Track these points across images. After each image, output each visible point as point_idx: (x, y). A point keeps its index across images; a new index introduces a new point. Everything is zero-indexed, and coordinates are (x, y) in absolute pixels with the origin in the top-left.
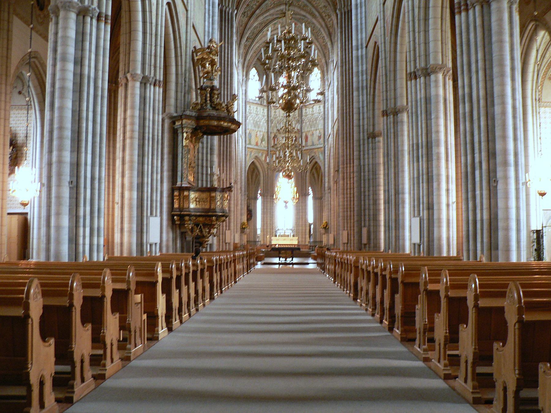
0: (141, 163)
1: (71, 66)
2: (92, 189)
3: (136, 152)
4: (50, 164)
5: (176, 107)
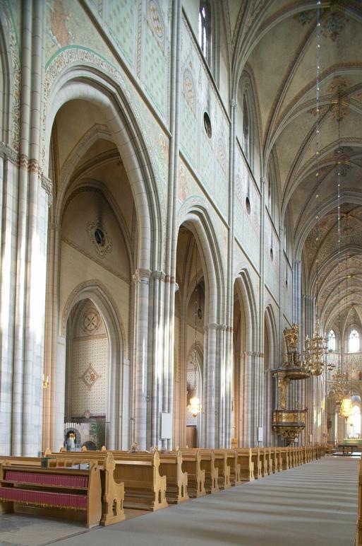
0: (253, 399)
1: (214, 356)
2: (226, 414)
3: (250, 393)
4: (206, 403)
5: (274, 365)
